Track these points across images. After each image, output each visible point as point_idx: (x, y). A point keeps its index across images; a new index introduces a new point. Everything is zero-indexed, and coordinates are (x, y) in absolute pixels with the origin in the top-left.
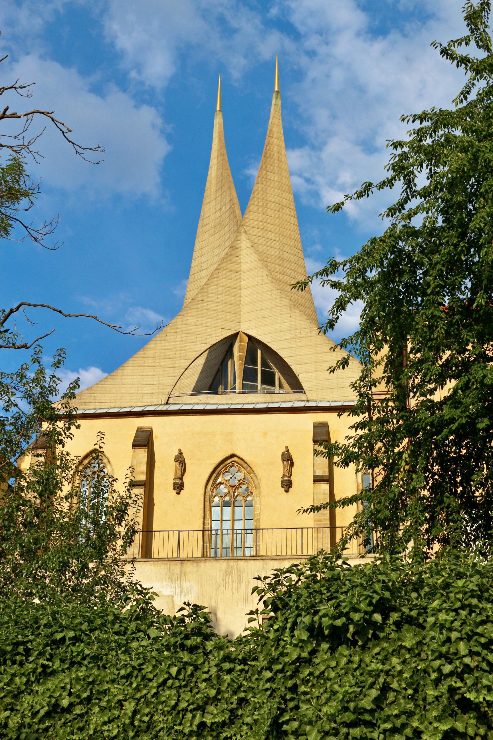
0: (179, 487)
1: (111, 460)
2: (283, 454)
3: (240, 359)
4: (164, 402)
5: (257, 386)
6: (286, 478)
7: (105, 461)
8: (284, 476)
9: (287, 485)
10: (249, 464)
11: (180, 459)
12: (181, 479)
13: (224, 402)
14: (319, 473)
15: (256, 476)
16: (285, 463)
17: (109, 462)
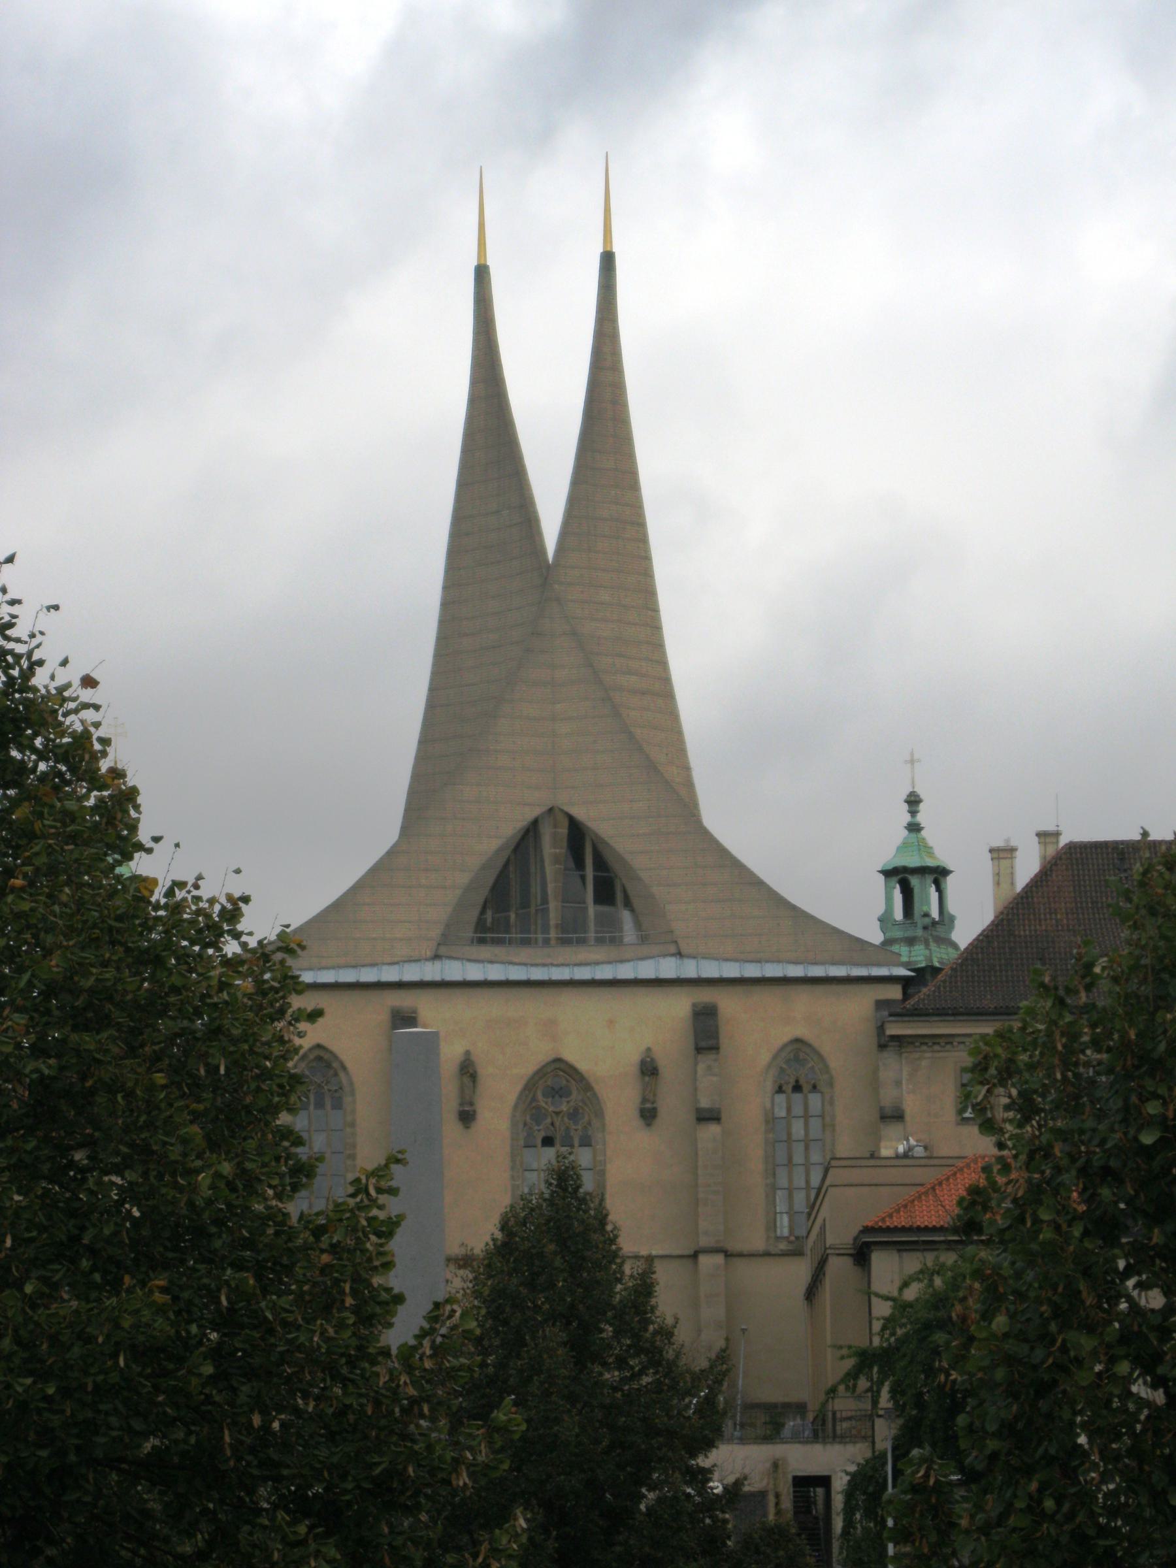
0: (467, 1117)
1: (348, 1065)
2: (643, 1063)
3: (556, 859)
4: (429, 954)
5: (586, 908)
6: (648, 1105)
7: (335, 1065)
8: (644, 1100)
9: (648, 1115)
10: (586, 1075)
11: (468, 1070)
12: (471, 1104)
13: (539, 961)
14: (704, 1103)
15: (595, 1094)
16: (647, 1079)
17: (344, 1068)
